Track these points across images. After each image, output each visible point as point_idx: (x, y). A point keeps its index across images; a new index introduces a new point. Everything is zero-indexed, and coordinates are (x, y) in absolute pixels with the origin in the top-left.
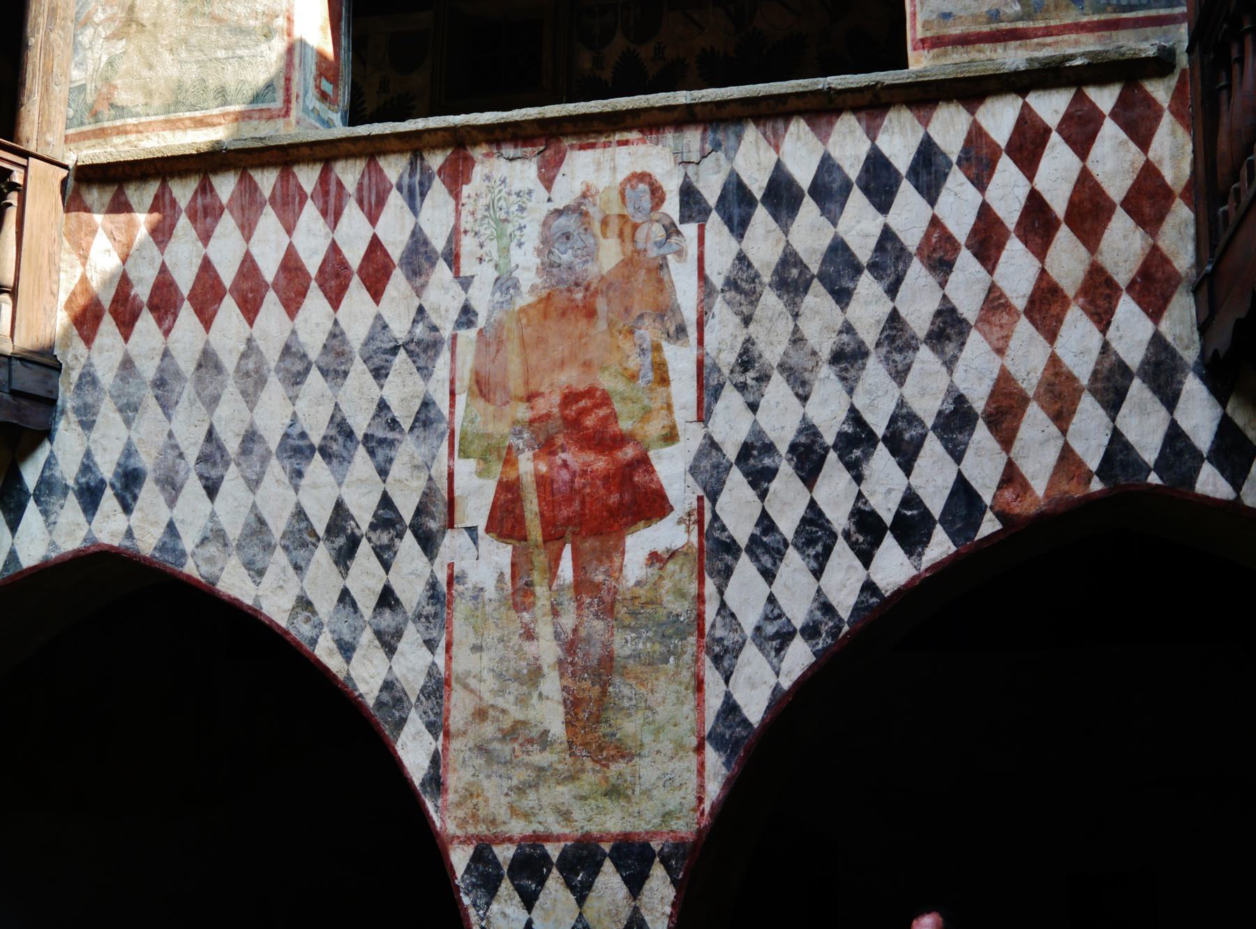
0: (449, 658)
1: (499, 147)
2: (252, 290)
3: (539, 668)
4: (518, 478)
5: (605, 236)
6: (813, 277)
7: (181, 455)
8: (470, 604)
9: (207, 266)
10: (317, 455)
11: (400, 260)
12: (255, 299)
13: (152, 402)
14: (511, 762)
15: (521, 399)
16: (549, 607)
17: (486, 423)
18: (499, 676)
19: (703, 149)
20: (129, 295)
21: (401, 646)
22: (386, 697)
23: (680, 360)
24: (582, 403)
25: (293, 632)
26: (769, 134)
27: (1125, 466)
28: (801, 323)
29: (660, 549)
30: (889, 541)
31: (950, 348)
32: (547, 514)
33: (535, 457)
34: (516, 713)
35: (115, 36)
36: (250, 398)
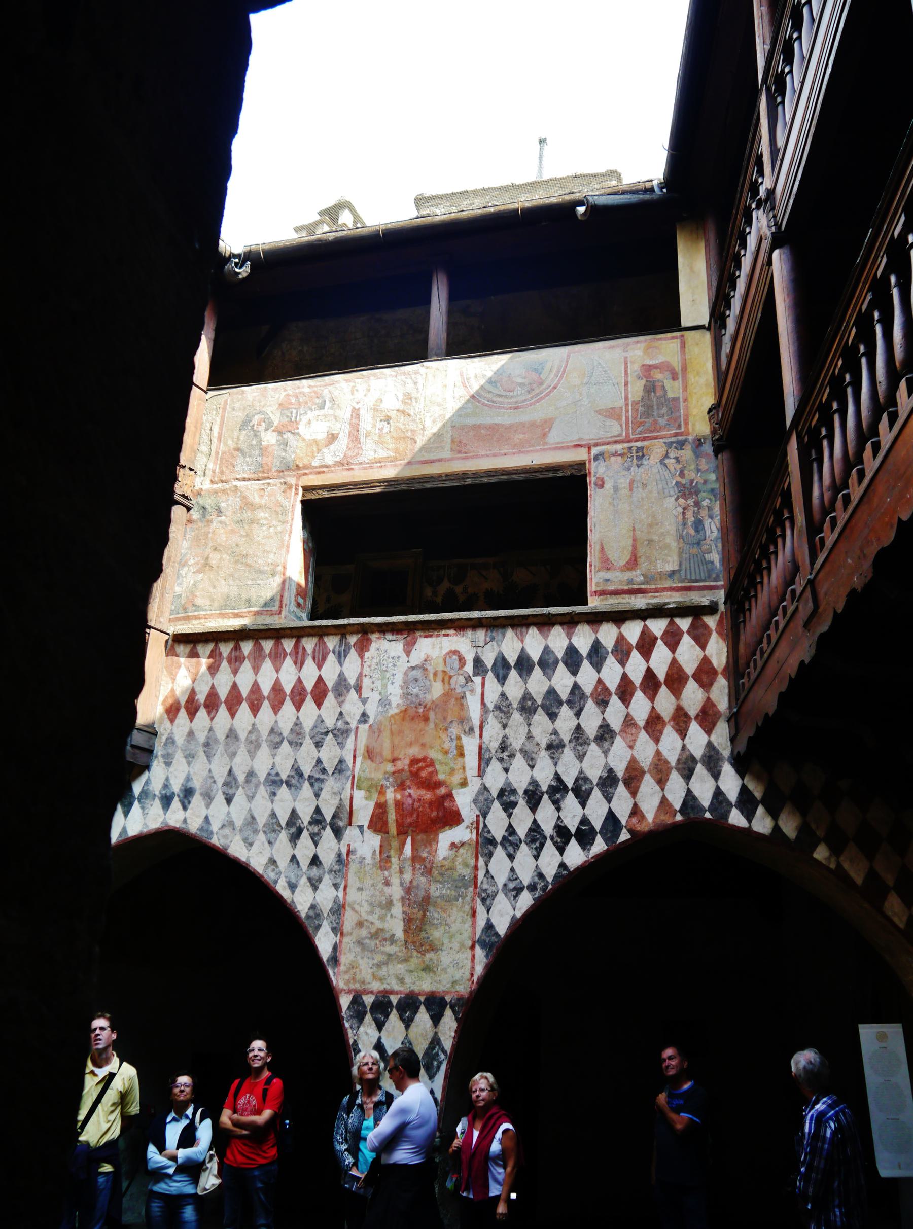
0: (345, 894)
1: (384, 634)
2: (257, 700)
3: (392, 901)
4: (386, 801)
5: (435, 681)
6: (538, 706)
7: (214, 782)
8: (358, 866)
9: (235, 686)
10: (284, 785)
12: (258, 704)
14: (374, 950)
15: (389, 761)
16: (398, 869)
17: (371, 772)
18: (371, 904)
19: (485, 640)
21: (321, 886)
22: (311, 913)
23: (471, 745)
24: (420, 765)
25: (266, 877)
26: (519, 634)
27: (693, 808)
28: (532, 728)
29: (457, 841)
30: (573, 841)
31: (606, 744)
32: (399, 821)
33: (395, 791)
34: (379, 924)
35: (198, 572)
36: (252, 754)
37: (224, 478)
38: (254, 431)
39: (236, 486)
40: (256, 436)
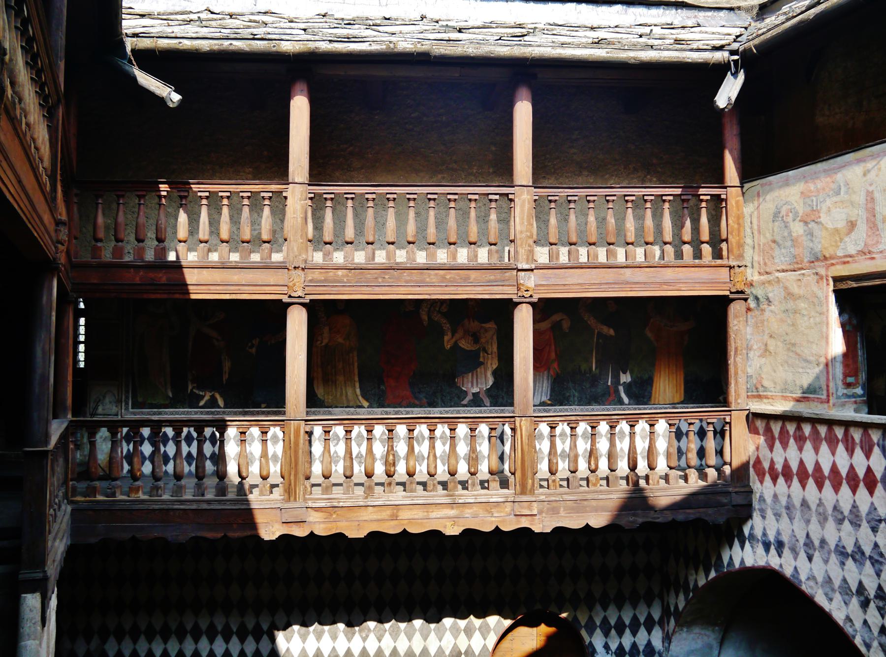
7: (797, 540)
10: (850, 558)
11: (881, 479)
13: (785, 515)
20: (774, 468)
37: (768, 270)
38: (784, 222)
39: (777, 278)
40: (786, 227)
